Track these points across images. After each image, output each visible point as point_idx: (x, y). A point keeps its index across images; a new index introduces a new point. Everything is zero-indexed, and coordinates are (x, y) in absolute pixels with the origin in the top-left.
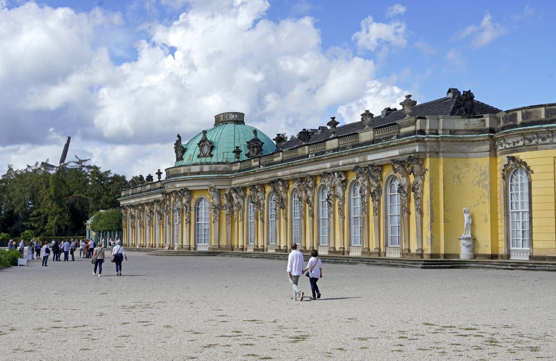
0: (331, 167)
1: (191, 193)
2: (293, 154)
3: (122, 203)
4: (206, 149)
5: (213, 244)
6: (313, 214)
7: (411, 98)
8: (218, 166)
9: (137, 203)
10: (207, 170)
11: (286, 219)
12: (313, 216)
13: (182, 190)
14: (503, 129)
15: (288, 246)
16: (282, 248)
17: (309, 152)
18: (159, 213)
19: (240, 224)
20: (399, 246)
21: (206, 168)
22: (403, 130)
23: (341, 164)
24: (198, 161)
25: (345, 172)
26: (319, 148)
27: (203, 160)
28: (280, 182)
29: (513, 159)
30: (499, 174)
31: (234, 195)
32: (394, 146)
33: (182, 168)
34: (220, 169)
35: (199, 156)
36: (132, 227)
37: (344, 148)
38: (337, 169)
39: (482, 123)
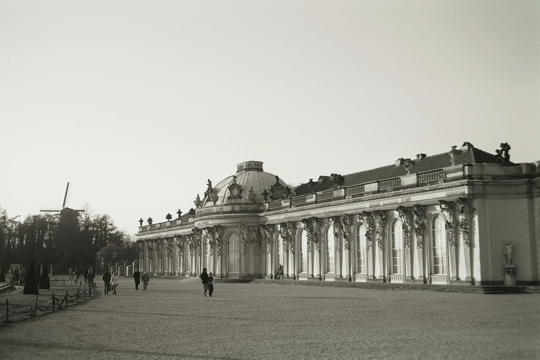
0: (371, 207)
4: (236, 192)
5: (243, 272)
7: (456, 149)
8: (247, 206)
9: (155, 238)
13: (214, 226)
17: (345, 194)
18: (179, 246)
21: (237, 208)
22: (449, 176)
23: (381, 204)
25: (386, 212)
31: (262, 231)
32: (442, 189)
33: (215, 208)
34: (250, 209)
36: (149, 258)
38: (377, 208)
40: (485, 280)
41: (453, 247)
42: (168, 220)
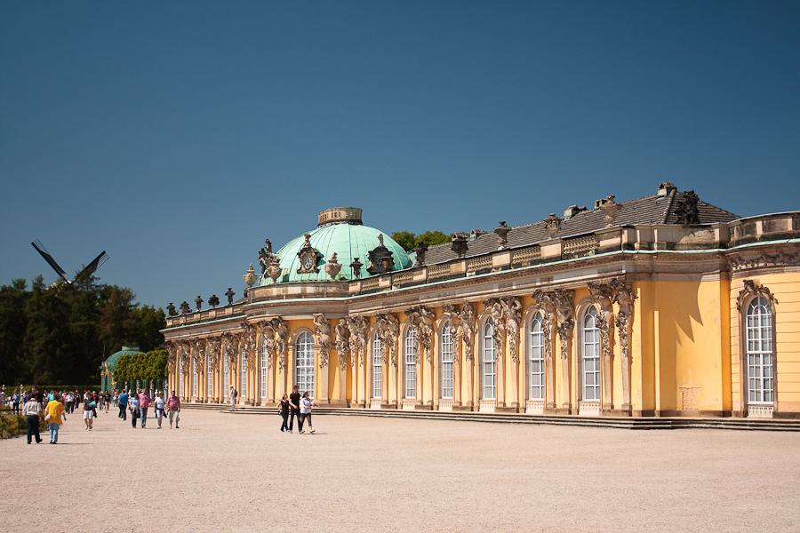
1: (287, 323)
2: (442, 271)
3: (167, 339)
4: (311, 261)
6: (472, 355)
10: (312, 292)
11: (432, 363)
12: (472, 358)
14: (738, 243)
15: (435, 401)
16: (425, 404)
17: (467, 269)
19: (361, 369)
20: (598, 400)
21: (310, 290)
22: (604, 243)
24: (298, 278)
26: (483, 264)
27: (305, 277)
28: (424, 311)
29: (750, 283)
30: (733, 303)
35: (299, 272)
36: (184, 373)
37: (519, 265)
39: (710, 235)
40: (646, 409)
41: (608, 357)
42: (211, 307)
